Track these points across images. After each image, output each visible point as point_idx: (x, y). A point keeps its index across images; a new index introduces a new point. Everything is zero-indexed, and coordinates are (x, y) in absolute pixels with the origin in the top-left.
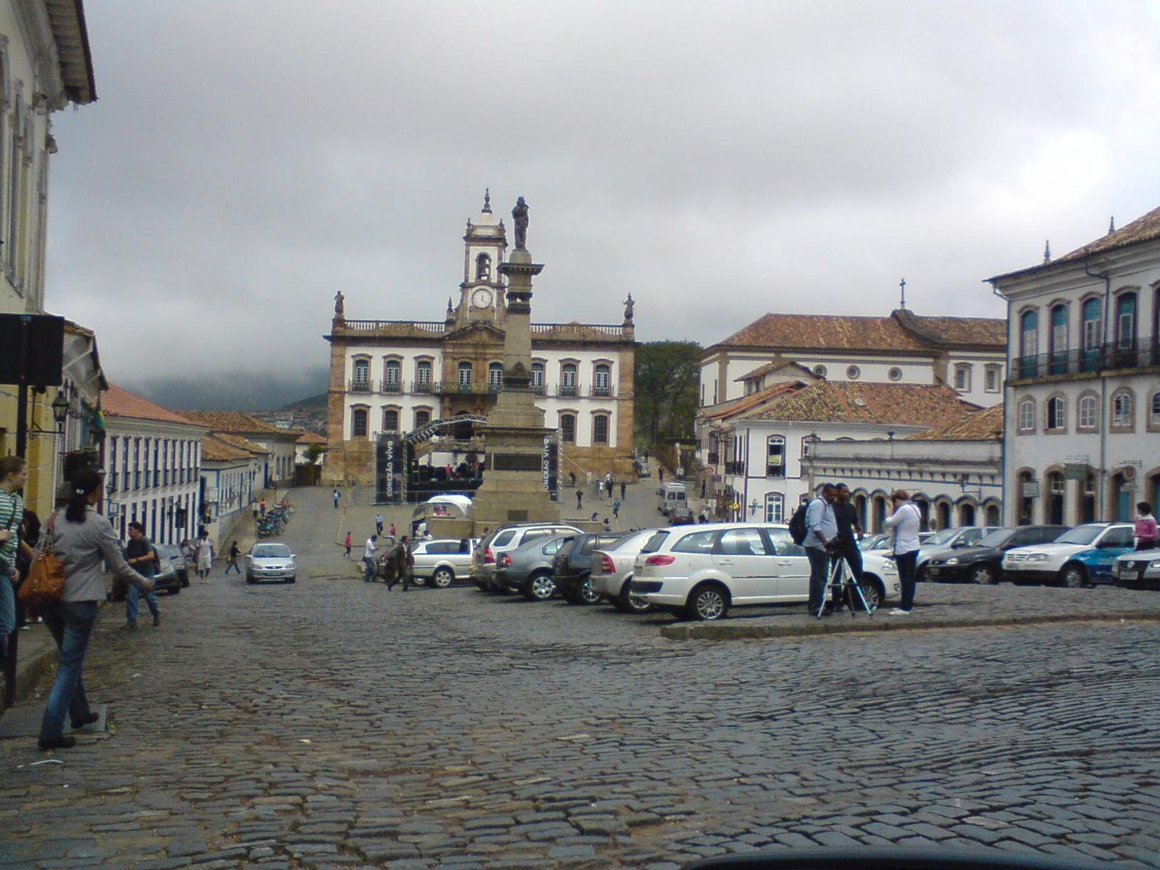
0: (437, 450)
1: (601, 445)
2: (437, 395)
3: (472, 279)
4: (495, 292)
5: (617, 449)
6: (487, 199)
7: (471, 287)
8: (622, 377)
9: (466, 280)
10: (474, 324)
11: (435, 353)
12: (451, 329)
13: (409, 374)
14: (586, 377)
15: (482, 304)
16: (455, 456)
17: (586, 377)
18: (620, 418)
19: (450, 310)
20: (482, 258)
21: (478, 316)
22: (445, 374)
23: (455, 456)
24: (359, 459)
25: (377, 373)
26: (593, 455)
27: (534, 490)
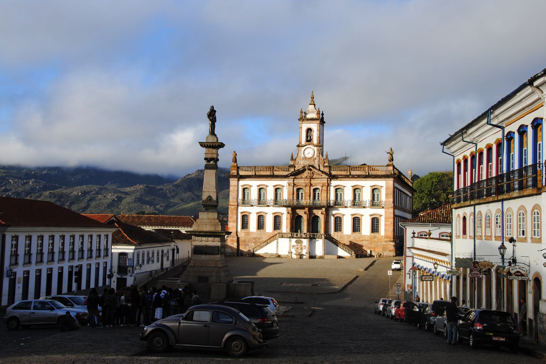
0: (282, 237)
1: (375, 234)
2: (284, 206)
3: (304, 142)
4: (316, 148)
5: (386, 237)
6: (313, 98)
7: (302, 146)
8: (387, 195)
9: (300, 143)
10: (304, 167)
11: (284, 183)
12: (292, 170)
13: (270, 195)
14: (366, 196)
15: (310, 156)
16: (290, 241)
17: (366, 196)
18: (386, 218)
19: (292, 159)
20: (309, 130)
21: (307, 163)
22: (289, 194)
23: (290, 241)
24: (245, 241)
25: (254, 195)
26: (371, 239)
27: (214, 265)
